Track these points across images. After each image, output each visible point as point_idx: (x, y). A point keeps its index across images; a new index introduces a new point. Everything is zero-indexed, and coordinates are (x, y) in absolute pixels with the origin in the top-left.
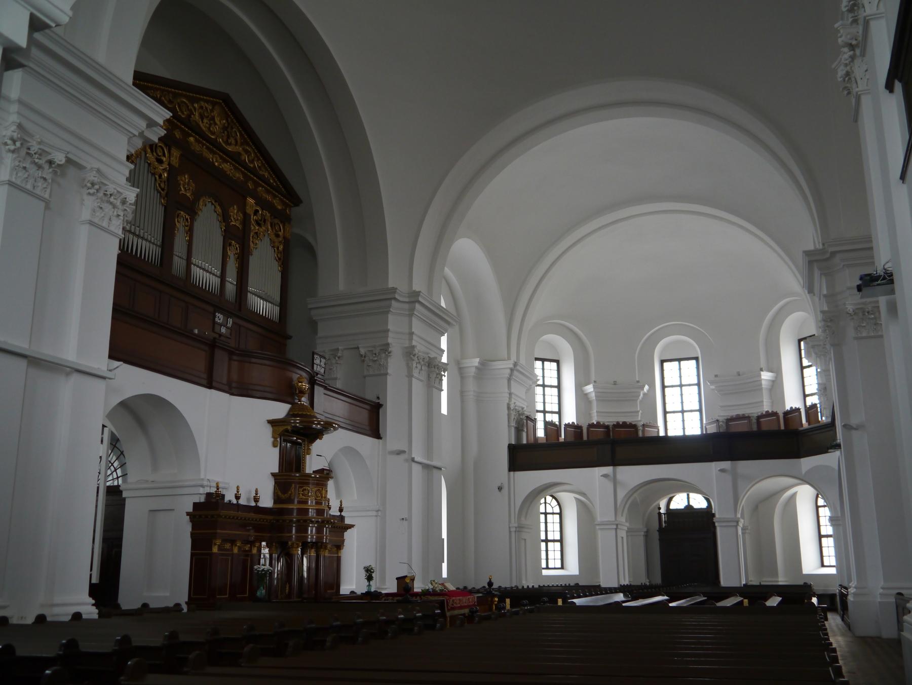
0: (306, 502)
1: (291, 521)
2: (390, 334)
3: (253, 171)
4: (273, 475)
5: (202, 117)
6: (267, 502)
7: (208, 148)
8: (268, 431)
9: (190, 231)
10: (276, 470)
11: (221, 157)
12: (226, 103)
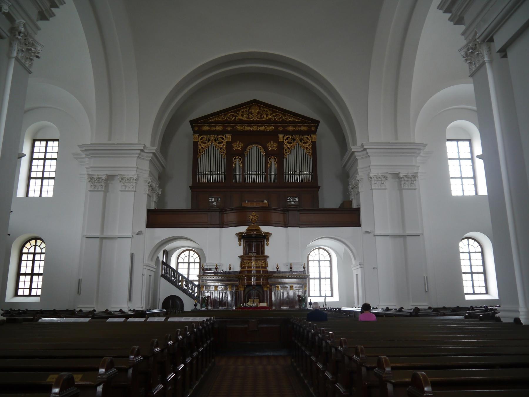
0: (251, 268)
1: (251, 276)
2: (359, 170)
3: (283, 122)
4: (240, 257)
5: (243, 116)
6: (237, 268)
7: (248, 126)
8: (237, 239)
9: (243, 163)
10: (242, 254)
11: (257, 126)
12: (255, 103)
